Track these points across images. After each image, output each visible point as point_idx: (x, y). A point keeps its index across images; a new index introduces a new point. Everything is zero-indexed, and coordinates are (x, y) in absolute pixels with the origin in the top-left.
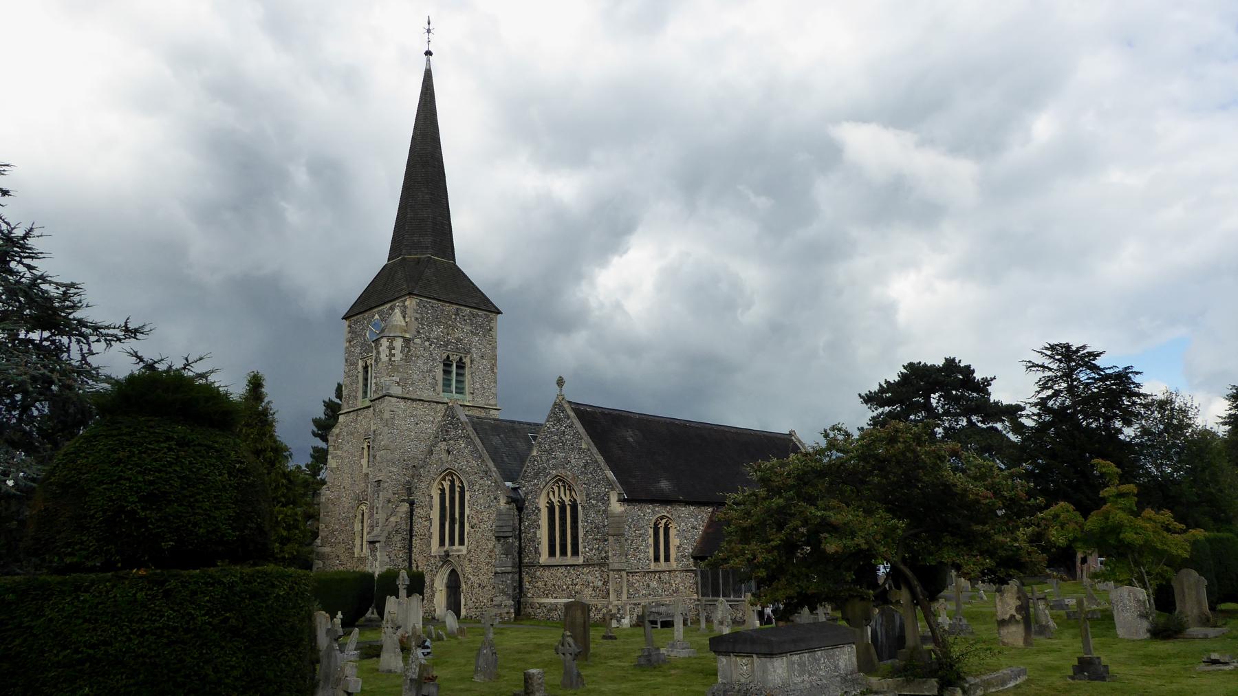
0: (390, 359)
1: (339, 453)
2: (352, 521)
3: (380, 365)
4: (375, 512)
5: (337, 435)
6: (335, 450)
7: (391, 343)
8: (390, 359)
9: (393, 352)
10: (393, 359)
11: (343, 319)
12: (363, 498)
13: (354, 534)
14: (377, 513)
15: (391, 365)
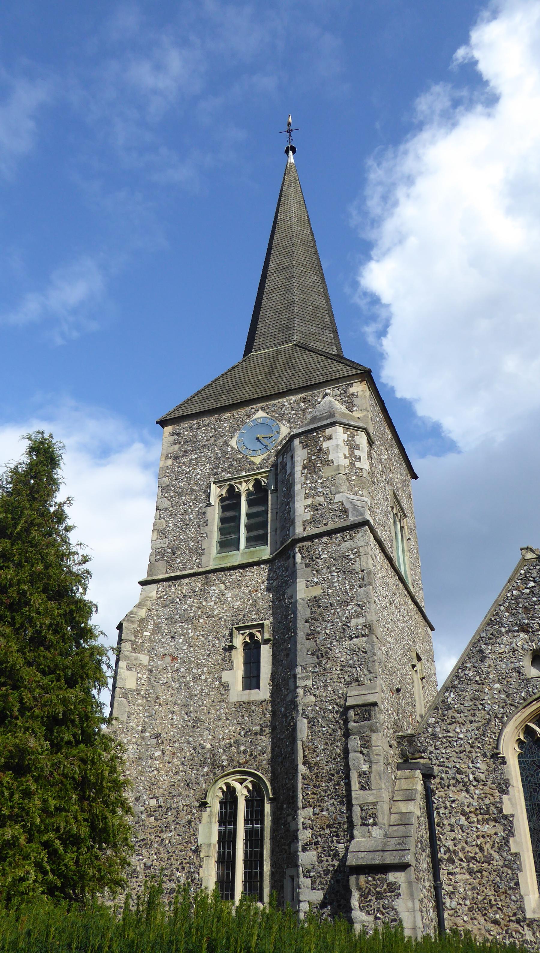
0: (353, 465)
1: (144, 659)
2: (184, 818)
3: (326, 472)
4: (355, 785)
5: (141, 621)
6: (134, 650)
7: (352, 436)
8: (353, 465)
9: (356, 452)
10: (358, 465)
11: (157, 423)
12: (231, 760)
13: (197, 851)
14: (362, 788)
15: (356, 474)
